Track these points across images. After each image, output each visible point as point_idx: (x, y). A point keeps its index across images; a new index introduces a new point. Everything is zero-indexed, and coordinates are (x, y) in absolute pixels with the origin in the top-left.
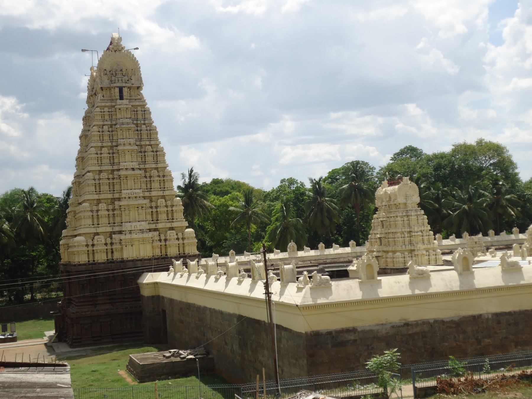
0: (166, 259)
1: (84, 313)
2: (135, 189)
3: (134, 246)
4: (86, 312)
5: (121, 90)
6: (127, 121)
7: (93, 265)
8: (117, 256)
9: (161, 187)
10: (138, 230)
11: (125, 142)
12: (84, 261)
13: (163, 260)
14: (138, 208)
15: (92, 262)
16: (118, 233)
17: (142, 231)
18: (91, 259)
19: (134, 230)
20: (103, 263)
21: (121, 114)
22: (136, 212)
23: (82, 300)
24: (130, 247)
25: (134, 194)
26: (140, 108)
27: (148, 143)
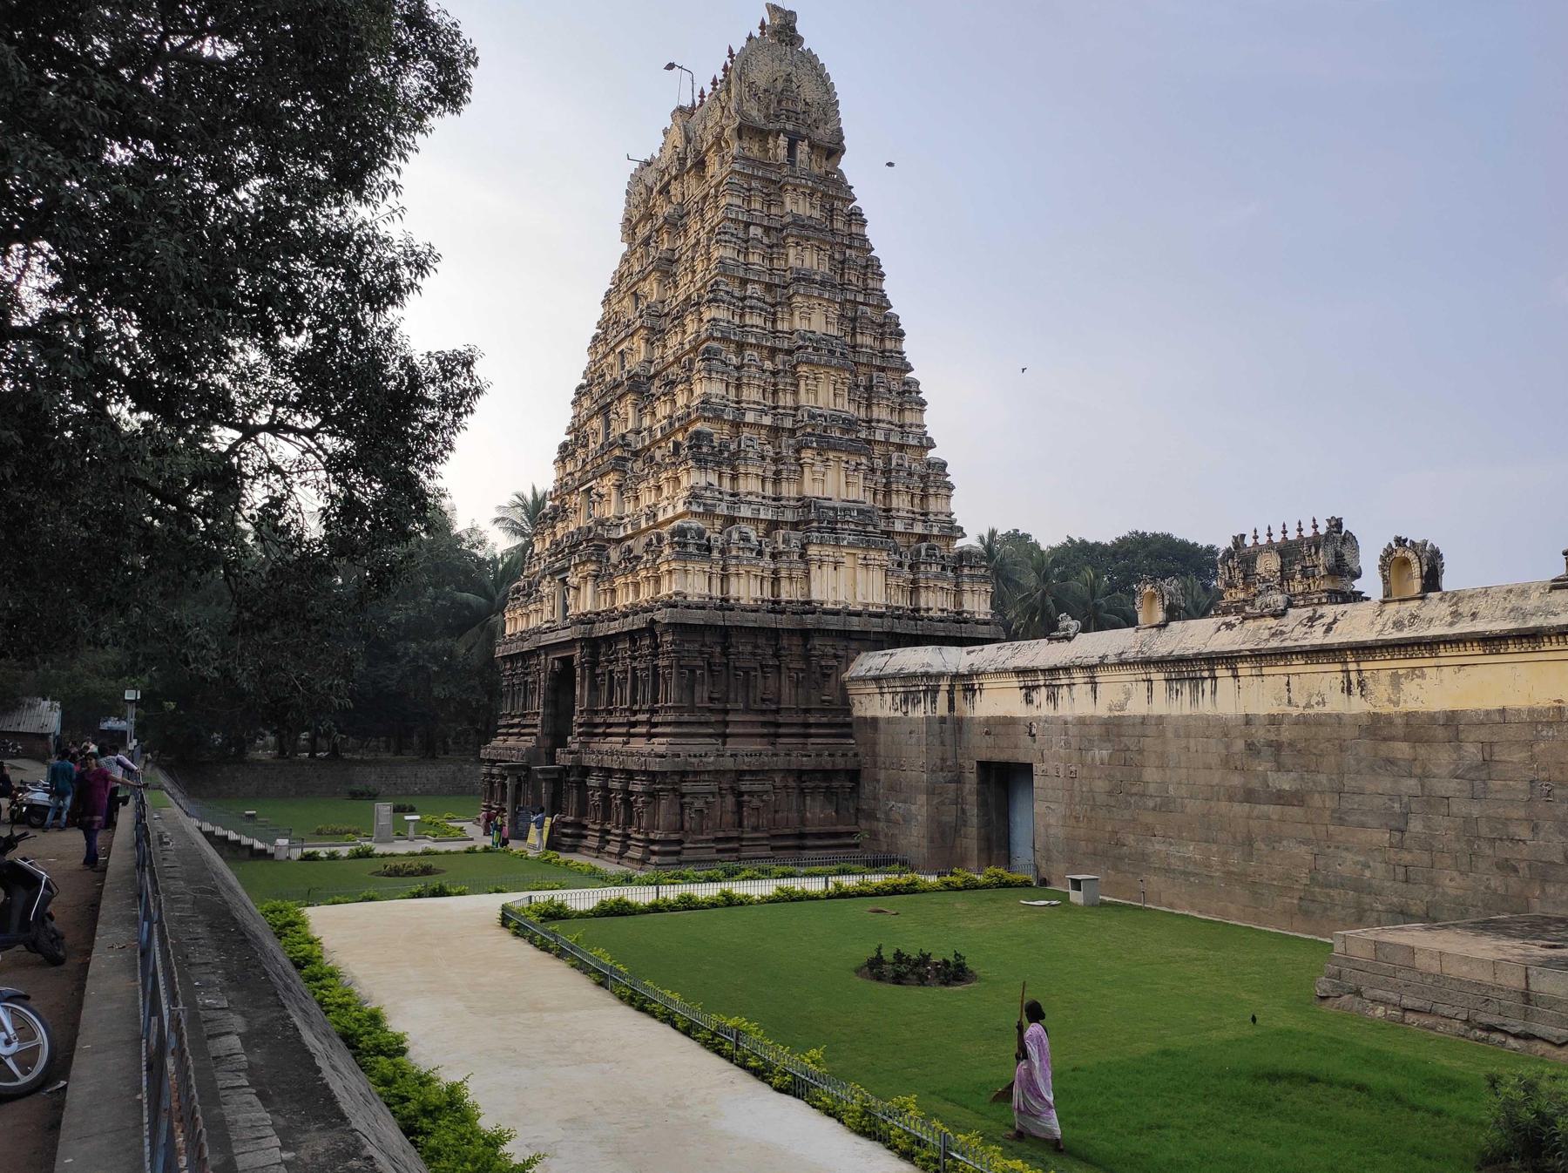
1: (693, 760)
3: (841, 569)
7: (727, 613)
8: (788, 592)
14: (847, 462)
22: (843, 474)
23: (686, 717)
24: (828, 569)
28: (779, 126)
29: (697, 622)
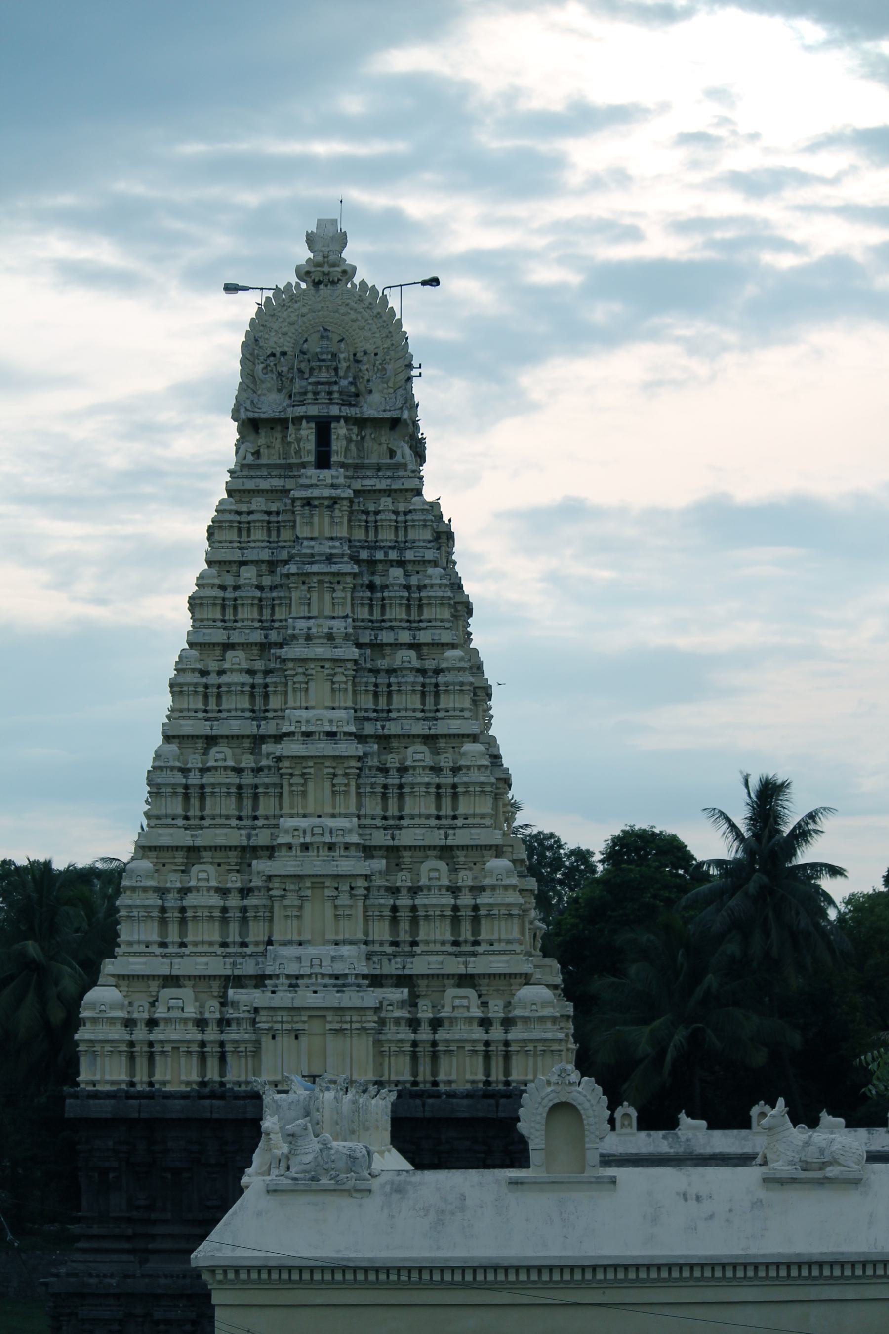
0: (430, 1101)
1: (93, 1281)
2: (333, 816)
4: (105, 1276)
5: (323, 429)
6: (331, 548)
7: (144, 1101)
9: (442, 813)
10: (323, 976)
11: (314, 631)
12: (113, 1083)
13: (418, 1101)
15: (501, 1087)
16: (254, 982)
17: (339, 981)
18: (141, 1076)
19: (309, 976)
20: (469, 1095)
21: (311, 524)
22: (329, 905)
23: (96, 1230)
24: (285, 1041)
25: (322, 834)
26: (389, 499)
27: (405, 637)
28: (300, 411)
29: (104, 1116)
